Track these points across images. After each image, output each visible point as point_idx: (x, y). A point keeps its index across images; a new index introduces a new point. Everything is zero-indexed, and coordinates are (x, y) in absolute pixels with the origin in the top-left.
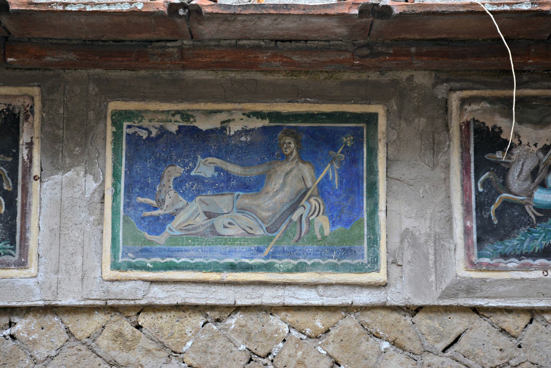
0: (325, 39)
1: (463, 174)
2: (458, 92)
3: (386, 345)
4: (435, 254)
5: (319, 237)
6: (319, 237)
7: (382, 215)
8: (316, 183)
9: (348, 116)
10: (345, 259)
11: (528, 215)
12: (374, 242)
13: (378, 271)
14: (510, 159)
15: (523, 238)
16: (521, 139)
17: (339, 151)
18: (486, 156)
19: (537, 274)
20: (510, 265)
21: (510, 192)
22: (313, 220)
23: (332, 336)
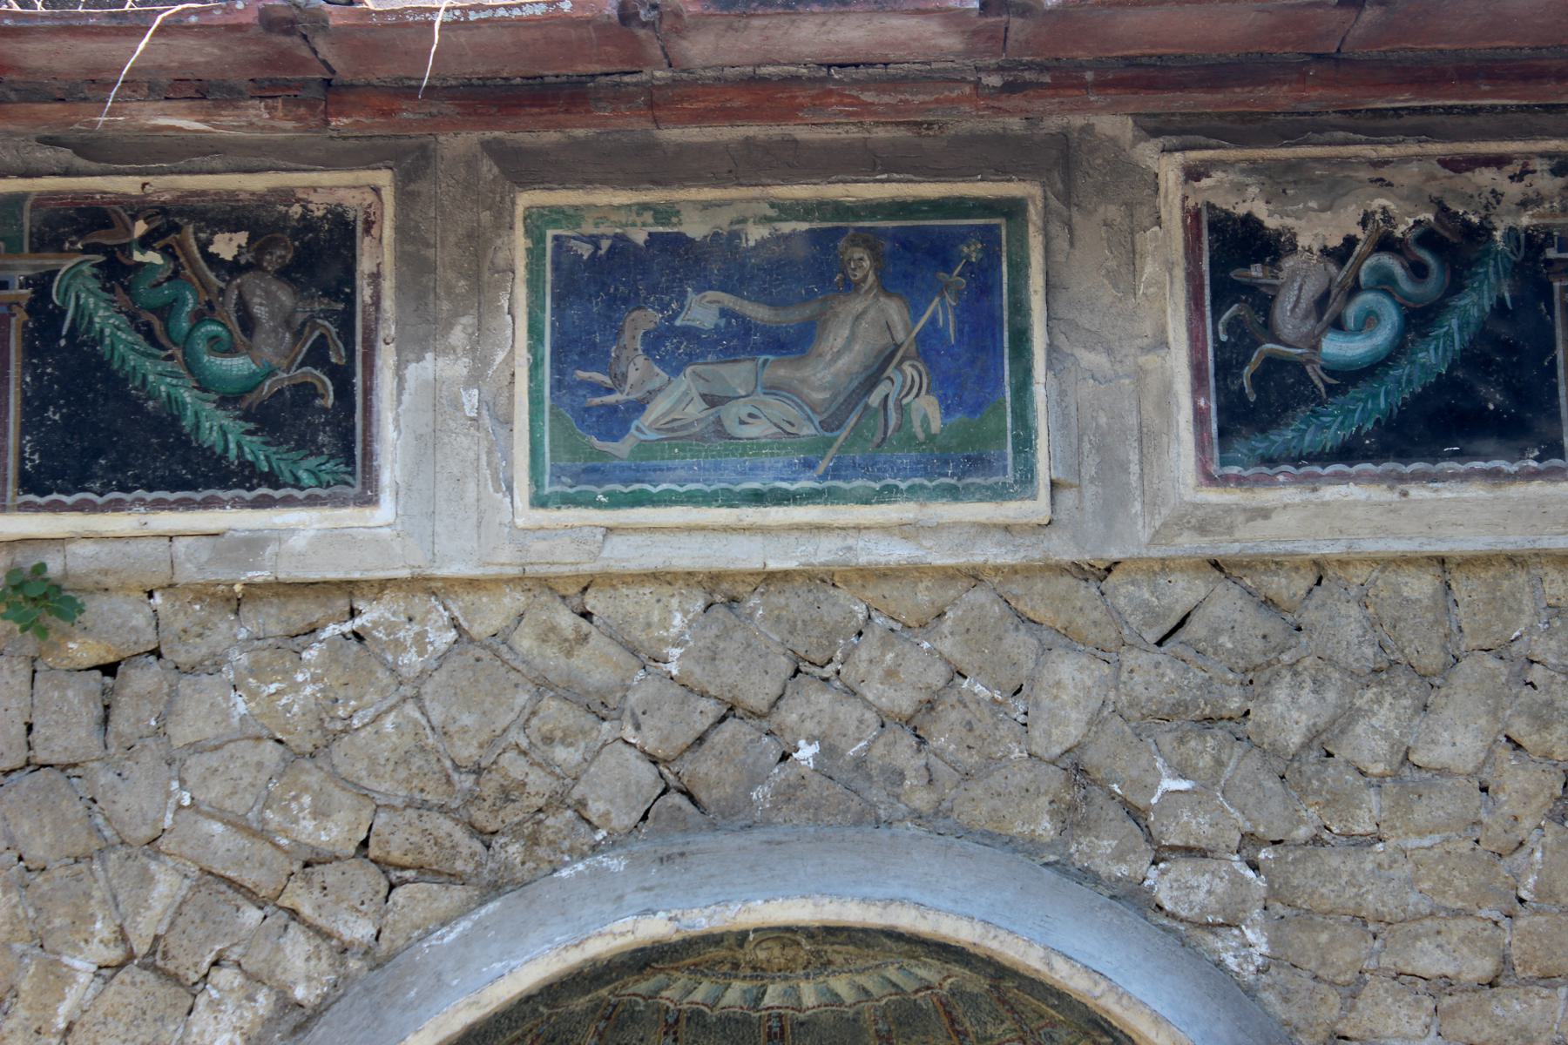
0: (921, 59)
4: (1141, 462)
5: (921, 436)
6: (921, 436)
7: (1039, 391)
8: (914, 334)
10: (970, 476)
11: (1312, 382)
12: (1025, 443)
13: (1034, 497)
14: (1277, 278)
15: (1303, 427)
17: (956, 272)
18: (1232, 275)
21: (1278, 341)
22: (908, 404)
23: (949, 623)
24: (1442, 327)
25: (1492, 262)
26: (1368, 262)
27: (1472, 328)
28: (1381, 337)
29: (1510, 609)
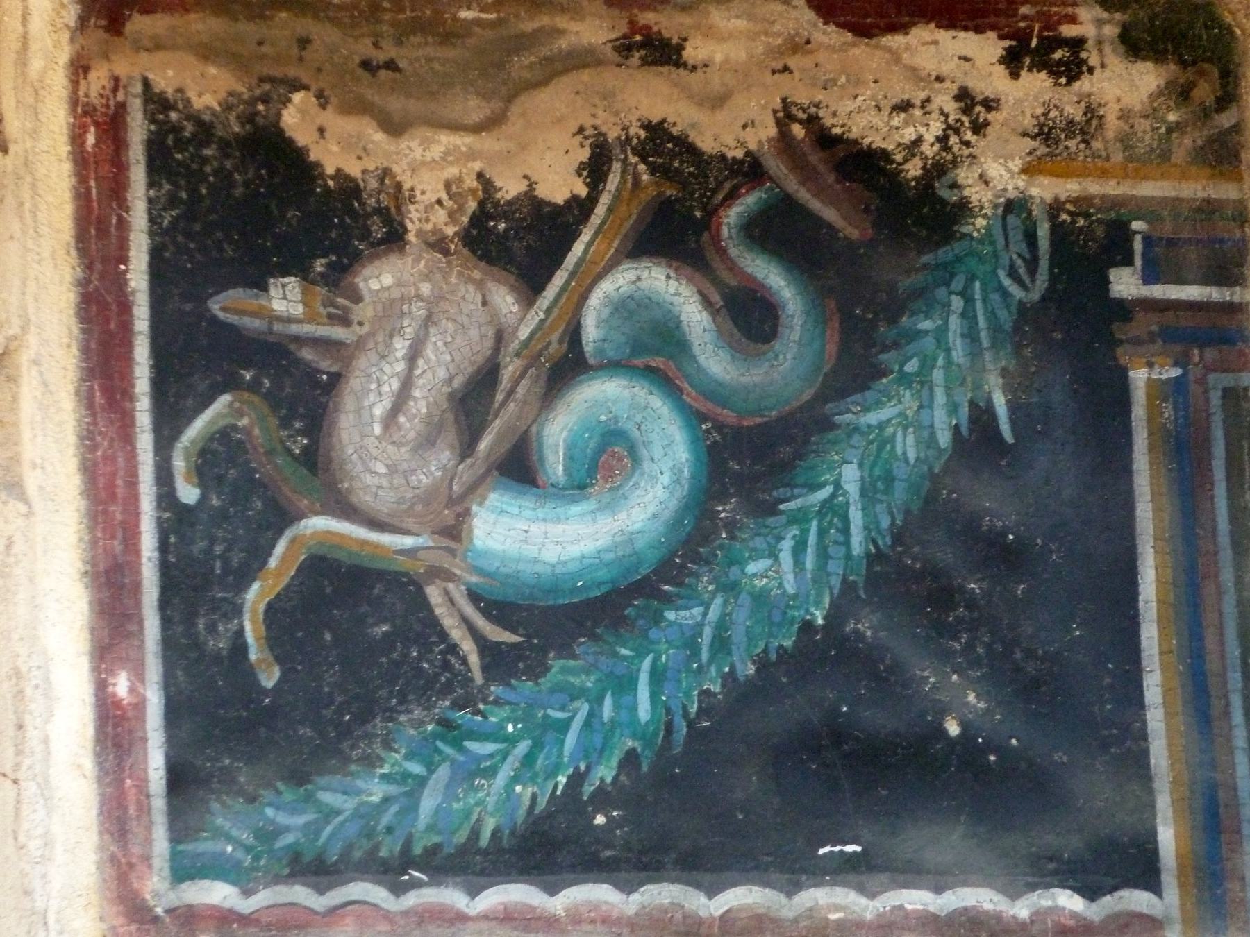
1: (90, 405)
11: (443, 635)
14: (345, 321)
15: (416, 768)
21: (348, 511)
24: (814, 487)
25: (957, 303)
27: (900, 492)
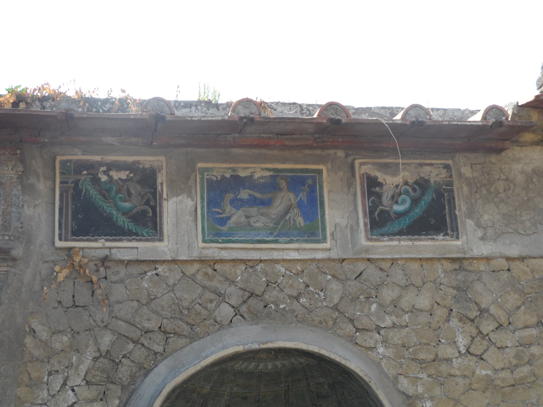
2: (358, 160)
3: (329, 277)
5: (299, 227)
8: (296, 202)
9: (309, 170)
10: (311, 237)
12: (324, 229)
15: (390, 227)
16: (386, 182)
19: (395, 243)
20: (385, 239)
21: (383, 206)
23: (305, 273)
26: (403, 188)
28: (407, 206)
29: (436, 271)
